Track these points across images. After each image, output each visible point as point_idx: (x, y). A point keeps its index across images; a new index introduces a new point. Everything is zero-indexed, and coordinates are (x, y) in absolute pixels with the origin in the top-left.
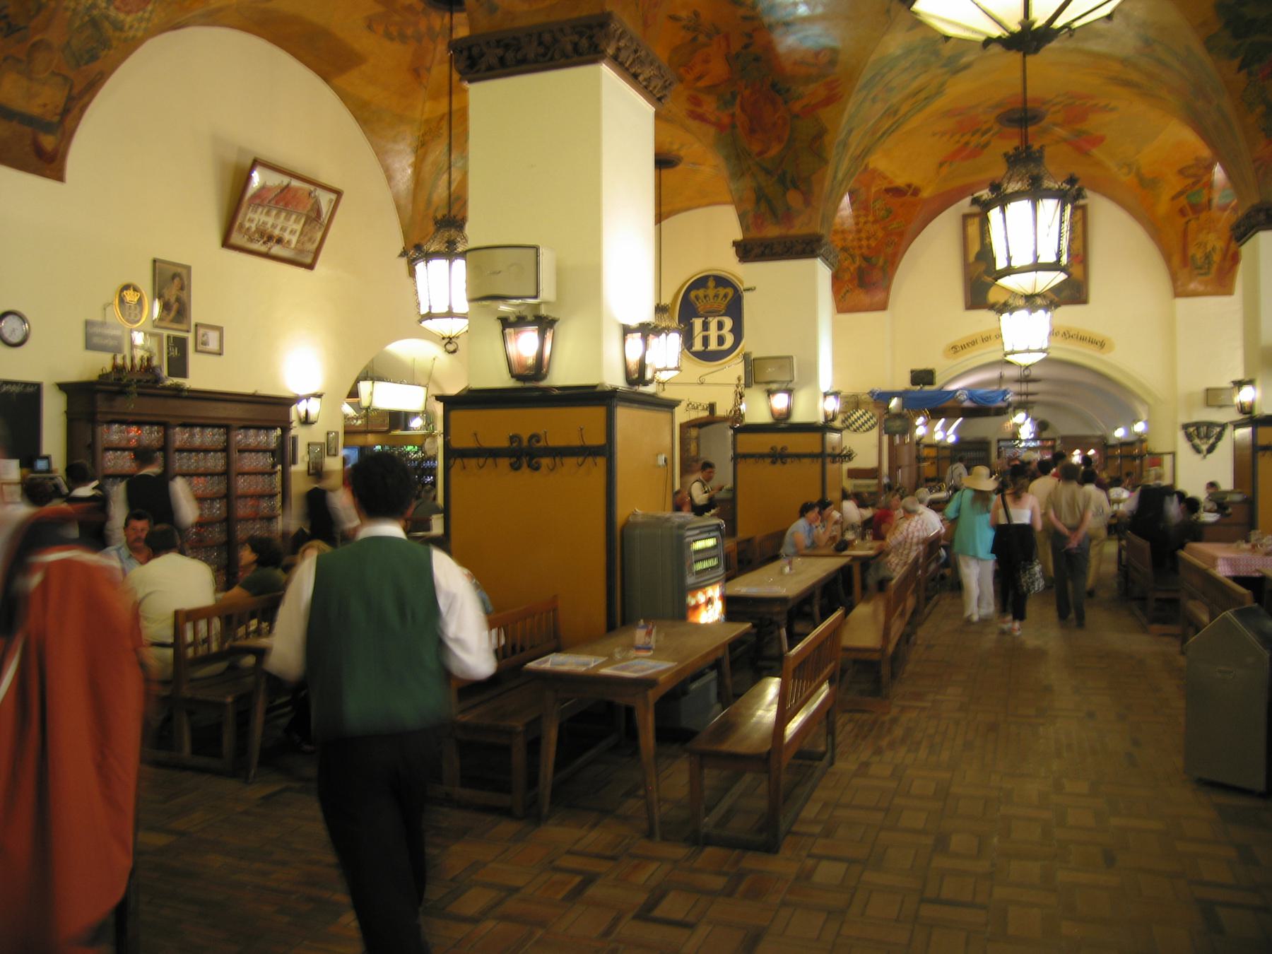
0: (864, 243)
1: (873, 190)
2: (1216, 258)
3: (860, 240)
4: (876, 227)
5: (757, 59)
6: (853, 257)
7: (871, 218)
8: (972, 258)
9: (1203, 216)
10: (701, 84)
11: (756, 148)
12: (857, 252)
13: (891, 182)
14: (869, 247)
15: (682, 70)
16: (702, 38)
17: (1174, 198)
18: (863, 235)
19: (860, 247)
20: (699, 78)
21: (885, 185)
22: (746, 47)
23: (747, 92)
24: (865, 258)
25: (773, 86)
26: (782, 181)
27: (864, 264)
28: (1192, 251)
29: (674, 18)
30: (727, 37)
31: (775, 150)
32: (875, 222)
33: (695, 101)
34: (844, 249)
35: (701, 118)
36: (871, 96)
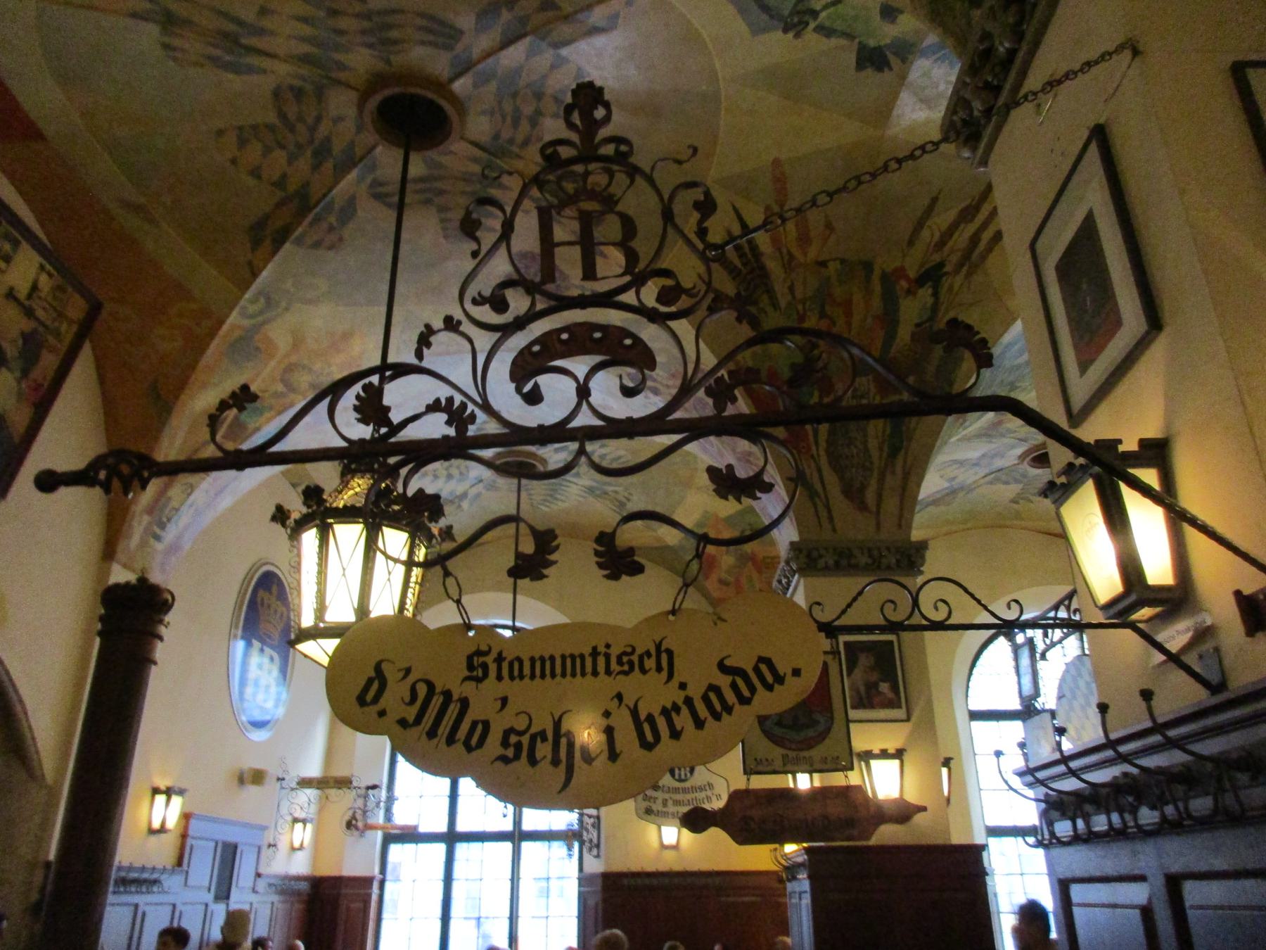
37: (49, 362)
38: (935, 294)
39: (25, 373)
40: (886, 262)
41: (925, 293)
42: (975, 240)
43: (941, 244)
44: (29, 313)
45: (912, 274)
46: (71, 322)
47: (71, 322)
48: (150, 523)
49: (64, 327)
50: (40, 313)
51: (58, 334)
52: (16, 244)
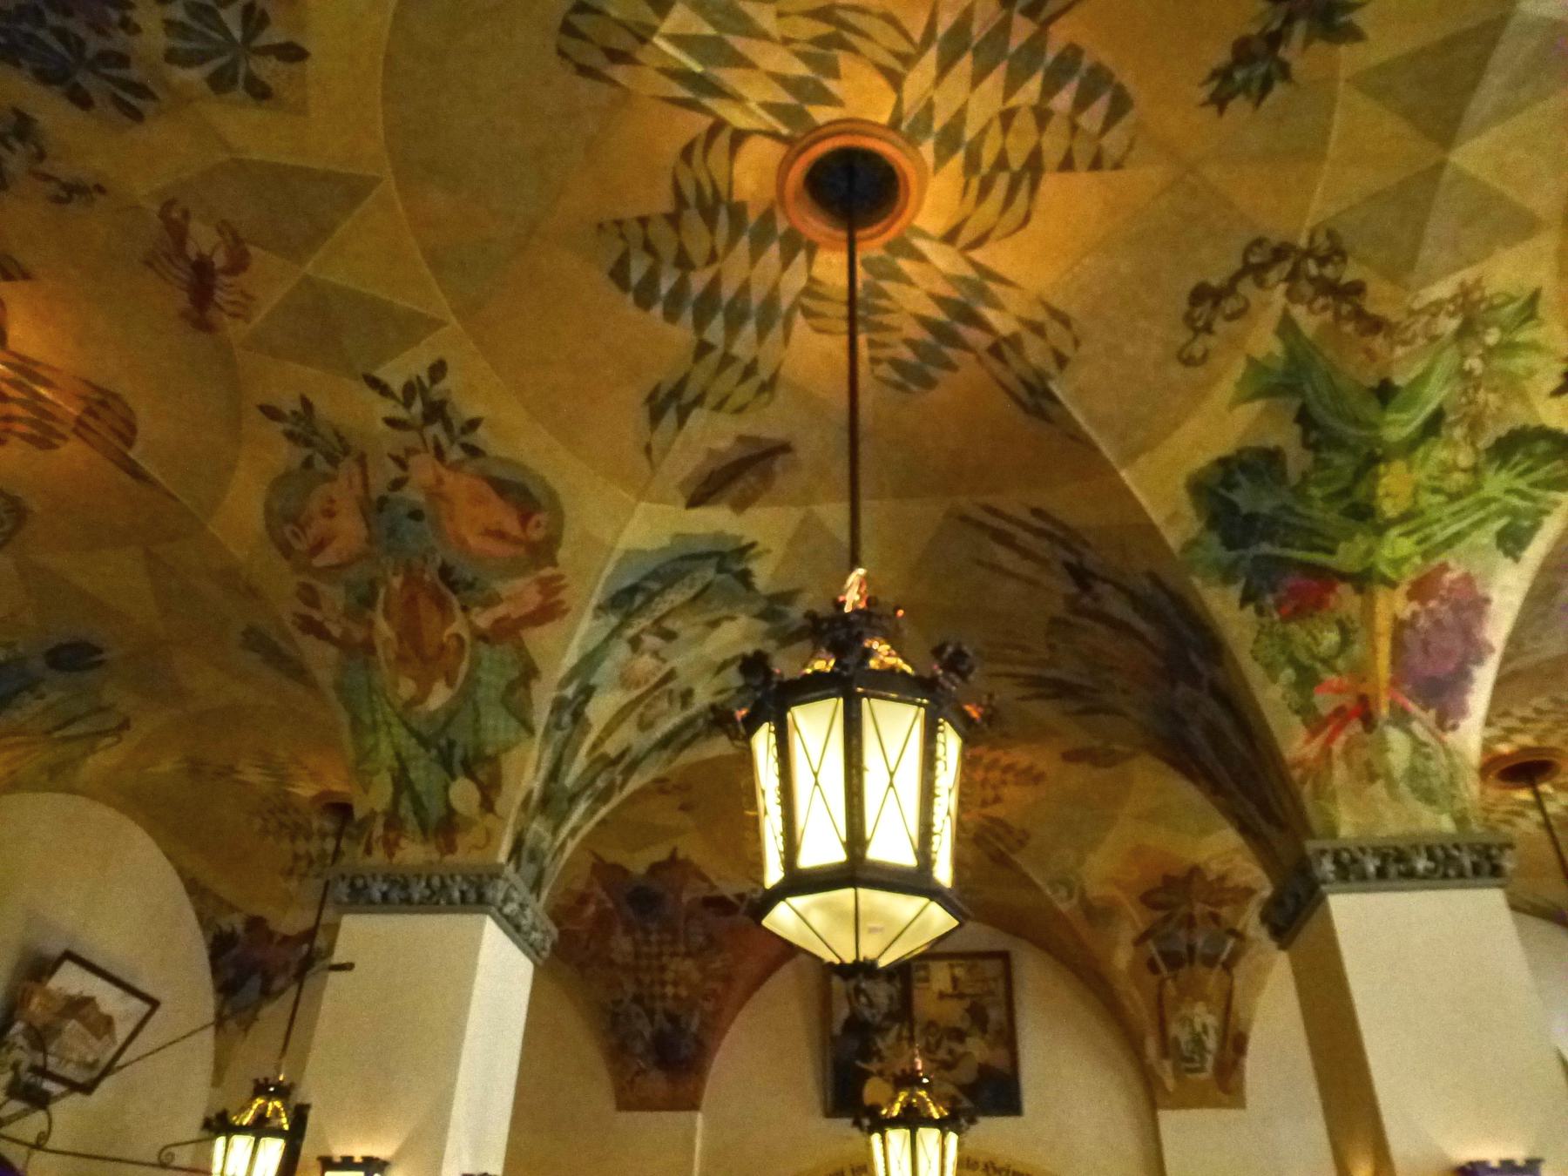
0: (670, 990)
1: (686, 898)
2: (1211, 1043)
3: (663, 984)
4: (688, 964)
5: (416, 515)
6: (651, 1013)
7: (682, 948)
8: (837, 1029)
9: (1183, 972)
10: (319, 562)
11: (407, 688)
12: (658, 1005)
13: (713, 887)
14: (676, 997)
15: (288, 529)
16: (321, 464)
17: (1140, 941)
18: (669, 976)
19: (663, 997)
20: (319, 546)
21: (703, 891)
22: (398, 484)
23: (397, 582)
24: (673, 1019)
25: (445, 572)
26: (446, 761)
27: (668, 1027)
28: (1175, 1029)
29: (271, 413)
30: (362, 460)
31: (439, 697)
32: (688, 955)
33: (310, 596)
34: (637, 999)
35: (319, 631)
36: (630, 632)
37: (995, 1015)
38: (1105, 580)
39: (984, 1031)
40: (1057, 608)
41: (1100, 588)
42: (1039, 533)
43: (1044, 563)
44: (961, 996)
45: (1073, 590)
46: (995, 980)
47: (995, 980)
48: (1175, 1068)
49: (993, 985)
50: (969, 991)
51: (991, 993)
52: (926, 968)
